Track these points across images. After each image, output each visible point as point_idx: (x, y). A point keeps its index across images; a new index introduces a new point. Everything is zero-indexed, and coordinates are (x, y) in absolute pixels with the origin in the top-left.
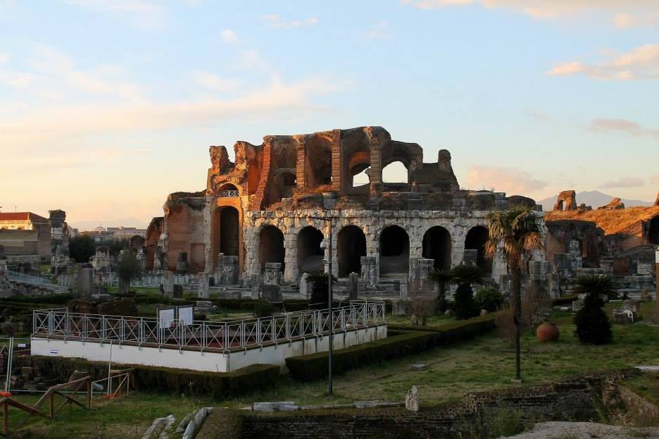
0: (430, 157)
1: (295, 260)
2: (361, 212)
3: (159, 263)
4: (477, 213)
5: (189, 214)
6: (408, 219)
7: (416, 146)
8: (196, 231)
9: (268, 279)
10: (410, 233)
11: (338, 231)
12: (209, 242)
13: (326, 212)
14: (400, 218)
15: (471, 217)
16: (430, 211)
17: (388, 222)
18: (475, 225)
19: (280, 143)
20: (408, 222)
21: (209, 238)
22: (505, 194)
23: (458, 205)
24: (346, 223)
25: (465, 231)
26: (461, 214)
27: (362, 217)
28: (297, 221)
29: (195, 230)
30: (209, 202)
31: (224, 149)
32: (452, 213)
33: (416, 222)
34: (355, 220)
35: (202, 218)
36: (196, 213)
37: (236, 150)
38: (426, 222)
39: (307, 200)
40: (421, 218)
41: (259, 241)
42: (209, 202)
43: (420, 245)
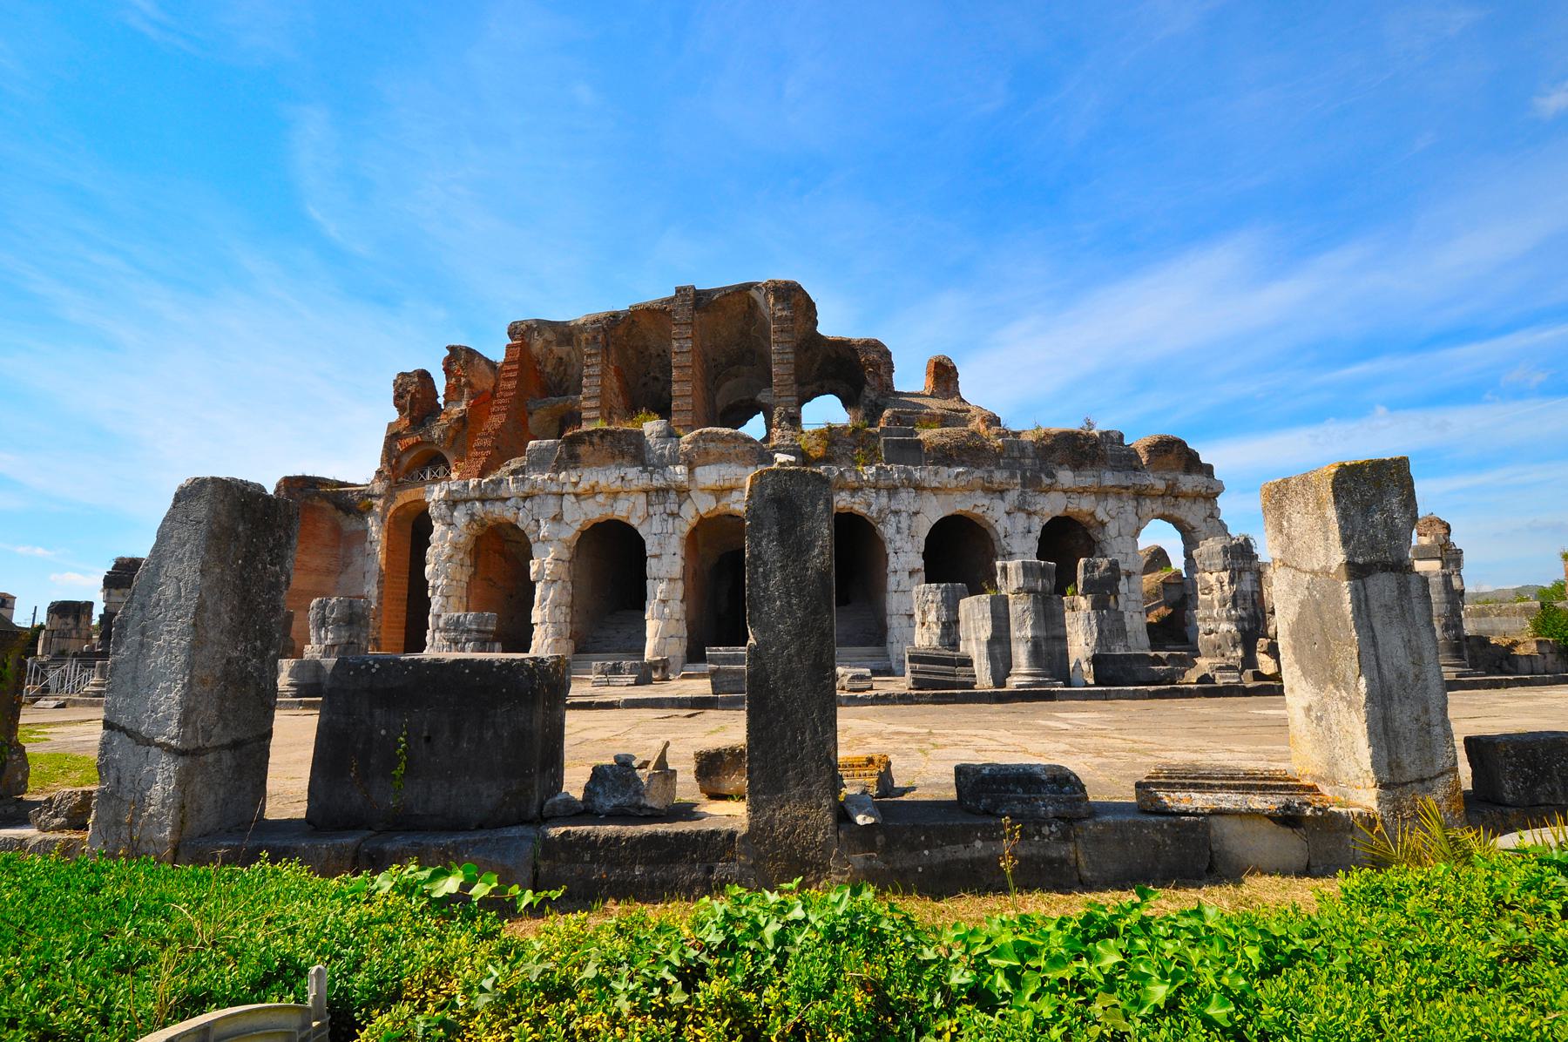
0: (910, 378)
1: (562, 615)
4: (1066, 477)
5: (337, 530)
6: (884, 493)
7: (876, 346)
8: (350, 569)
10: (888, 531)
11: (687, 529)
13: (651, 473)
14: (861, 489)
15: (1051, 488)
16: (944, 471)
18: (1059, 512)
19: (548, 342)
20: (884, 500)
21: (374, 581)
22: (1121, 436)
23: (1016, 454)
24: (705, 505)
25: (1037, 525)
26: (1023, 477)
28: (569, 501)
31: (424, 376)
32: (999, 476)
33: (906, 500)
36: (350, 524)
37: (448, 371)
40: (919, 488)
41: (468, 571)
43: (919, 563)
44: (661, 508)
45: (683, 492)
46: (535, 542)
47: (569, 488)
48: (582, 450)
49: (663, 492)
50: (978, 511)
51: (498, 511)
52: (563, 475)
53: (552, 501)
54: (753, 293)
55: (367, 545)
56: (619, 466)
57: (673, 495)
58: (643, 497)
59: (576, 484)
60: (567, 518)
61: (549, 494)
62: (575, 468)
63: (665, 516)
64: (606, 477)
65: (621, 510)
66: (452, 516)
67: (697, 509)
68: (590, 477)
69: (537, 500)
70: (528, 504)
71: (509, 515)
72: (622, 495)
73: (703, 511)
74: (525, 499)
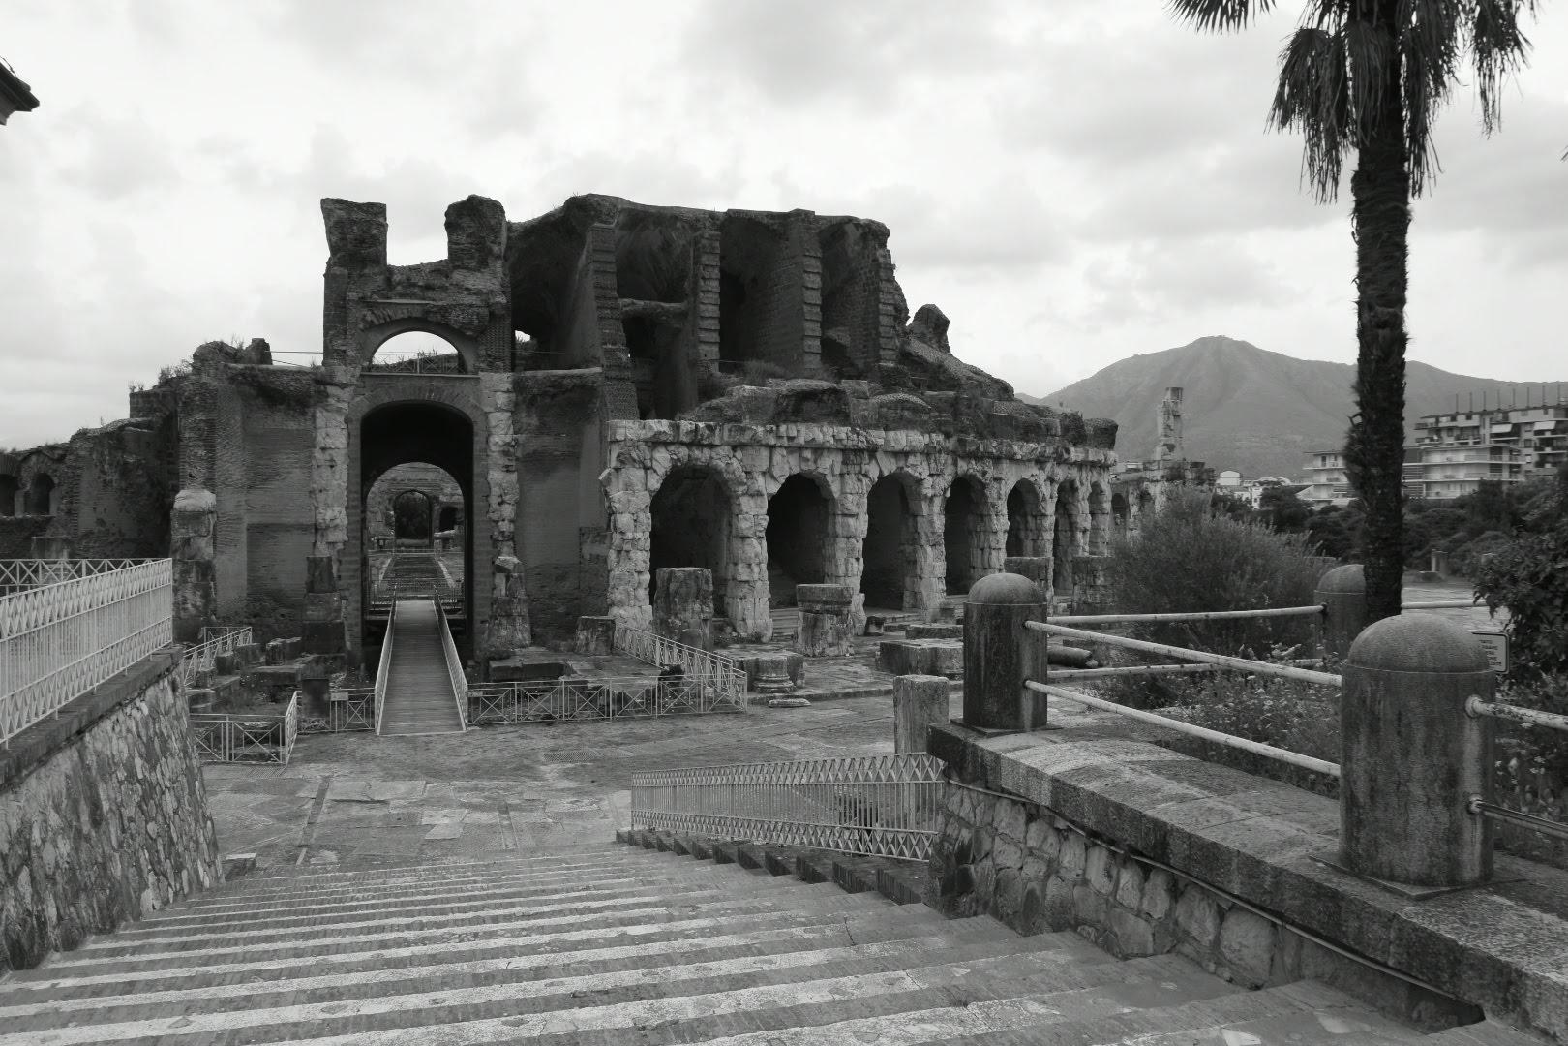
2: (927, 439)
3: (200, 602)
9: (830, 639)
10: (992, 493)
12: (343, 520)
17: (963, 466)
24: (889, 466)
27: (928, 453)
29: (268, 479)
30: (343, 386)
34: (911, 460)
35: (306, 442)
38: (1014, 468)
39: (825, 398)
40: (1012, 458)
42: (343, 386)
44: (857, 468)
45: (872, 451)
46: (744, 494)
47: (785, 442)
48: (809, 406)
49: (858, 451)
50: (1032, 480)
51: (702, 456)
52: (783, 428)
53: (765, 453)
54: (849, 228)
55: (318, 454)
56: (831, 424)
57: (866, 456)
58: (839, 458)
59: (791, 439)
60: (776, 472)
61: (761, 445)
62: (795, 422)
63: (861, 477)
64: (824, 433)
65: (828, 466)
66: (651, 460)
67: (881, 471)
68: (804, 433)
69: (751, 451)
70: (739, 455)
71: (722, 465)
72: (825, 453)
73: (886, 473)
74: (734, 448)
